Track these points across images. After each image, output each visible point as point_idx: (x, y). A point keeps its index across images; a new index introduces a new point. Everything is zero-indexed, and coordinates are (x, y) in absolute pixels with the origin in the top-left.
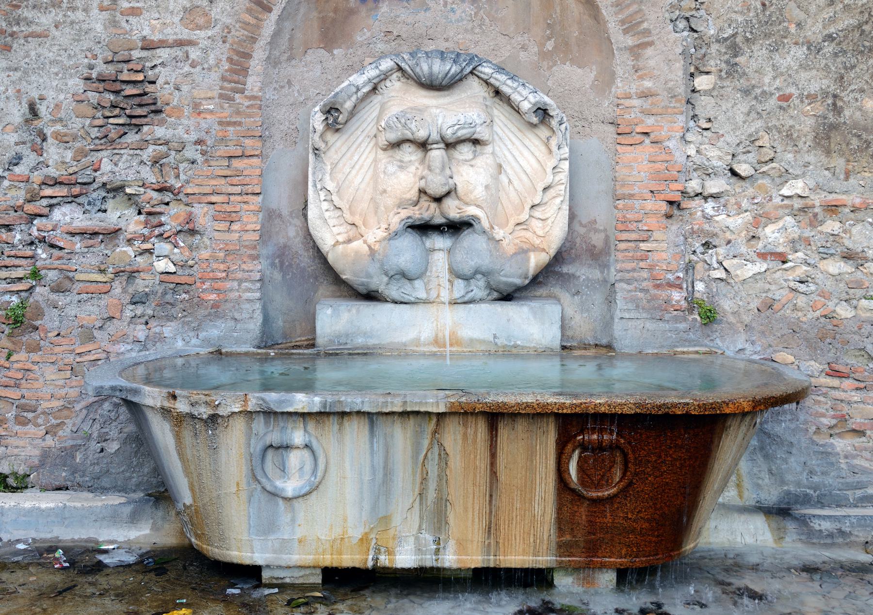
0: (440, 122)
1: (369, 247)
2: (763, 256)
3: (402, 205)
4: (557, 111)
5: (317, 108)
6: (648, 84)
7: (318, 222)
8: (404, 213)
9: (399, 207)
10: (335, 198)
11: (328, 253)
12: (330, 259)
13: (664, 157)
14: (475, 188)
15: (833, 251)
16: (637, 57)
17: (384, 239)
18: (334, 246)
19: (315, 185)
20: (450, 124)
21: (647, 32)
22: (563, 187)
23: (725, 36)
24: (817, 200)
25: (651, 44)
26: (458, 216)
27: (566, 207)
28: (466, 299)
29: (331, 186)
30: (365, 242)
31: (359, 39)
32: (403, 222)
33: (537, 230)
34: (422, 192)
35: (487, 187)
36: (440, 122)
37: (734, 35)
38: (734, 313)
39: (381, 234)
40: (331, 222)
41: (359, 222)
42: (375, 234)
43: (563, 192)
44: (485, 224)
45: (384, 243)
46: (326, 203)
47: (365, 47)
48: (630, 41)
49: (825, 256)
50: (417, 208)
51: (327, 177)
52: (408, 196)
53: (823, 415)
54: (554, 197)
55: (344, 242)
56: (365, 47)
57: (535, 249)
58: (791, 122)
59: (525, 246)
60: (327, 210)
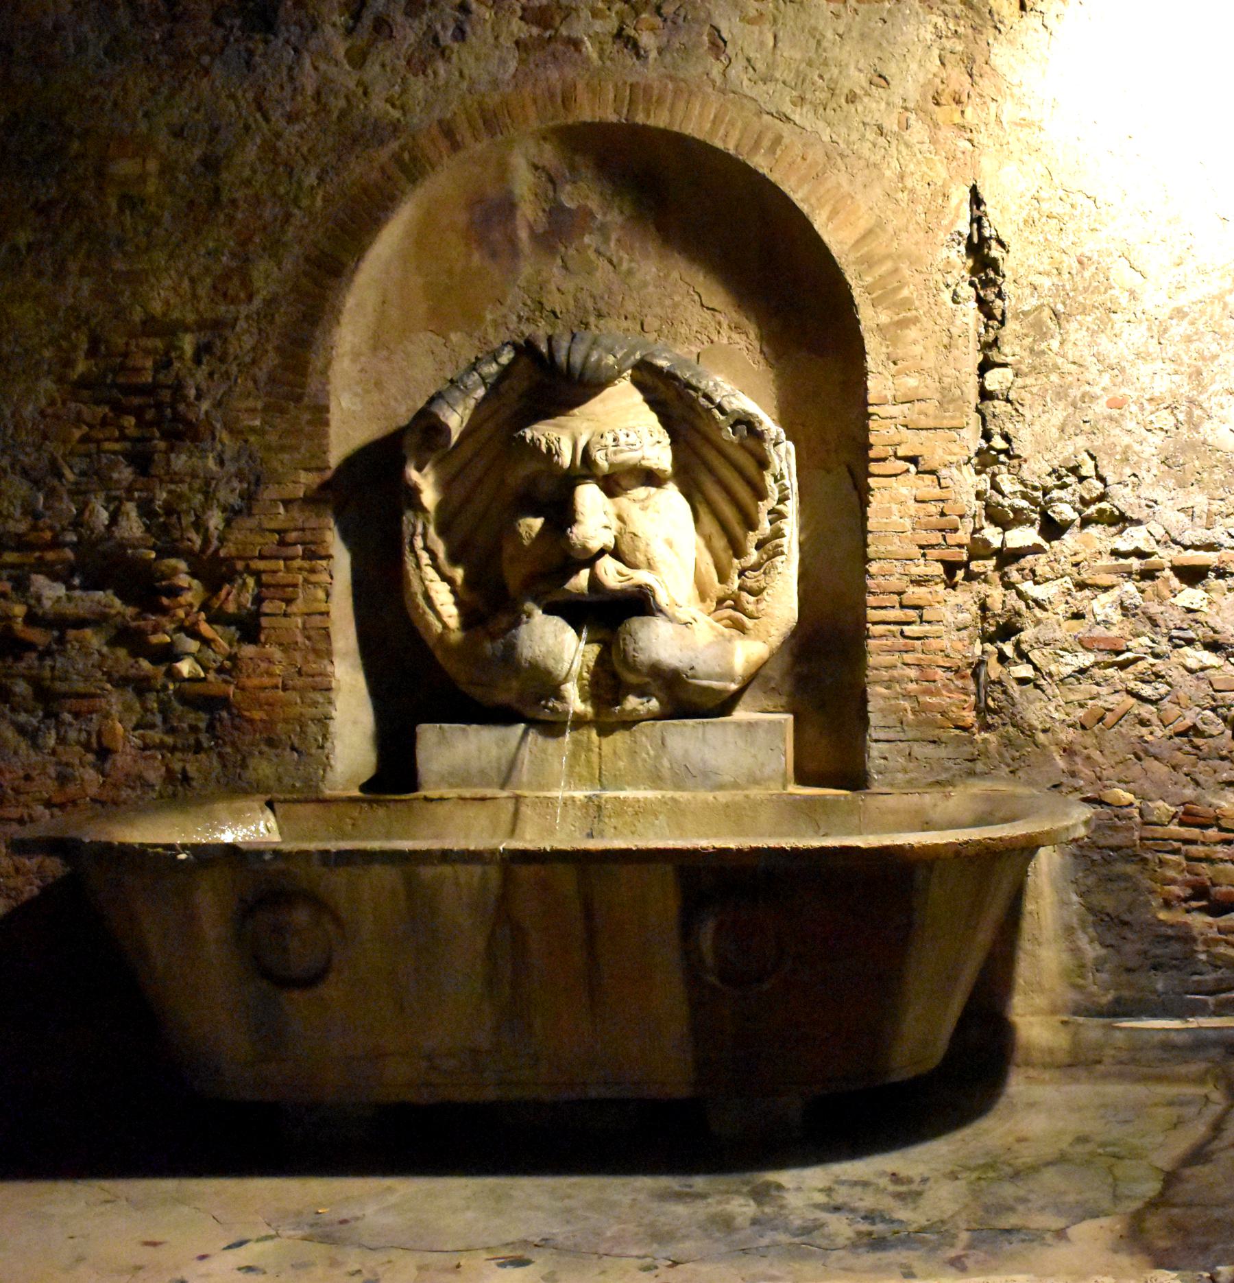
2: (1086, 645)
6: (912, 382)
13: (937, 492)
15: (1191, 634)
16: (895, 342)
21: (906, 304)
23: (1026, 308)
24: (1167, 556)
25: (916, 320)
37: (1039, 308)
38: (1045, 731)
48: (884, 318)
49: (1178, 643)
53: (1173, 882)
58: (1126, 440)
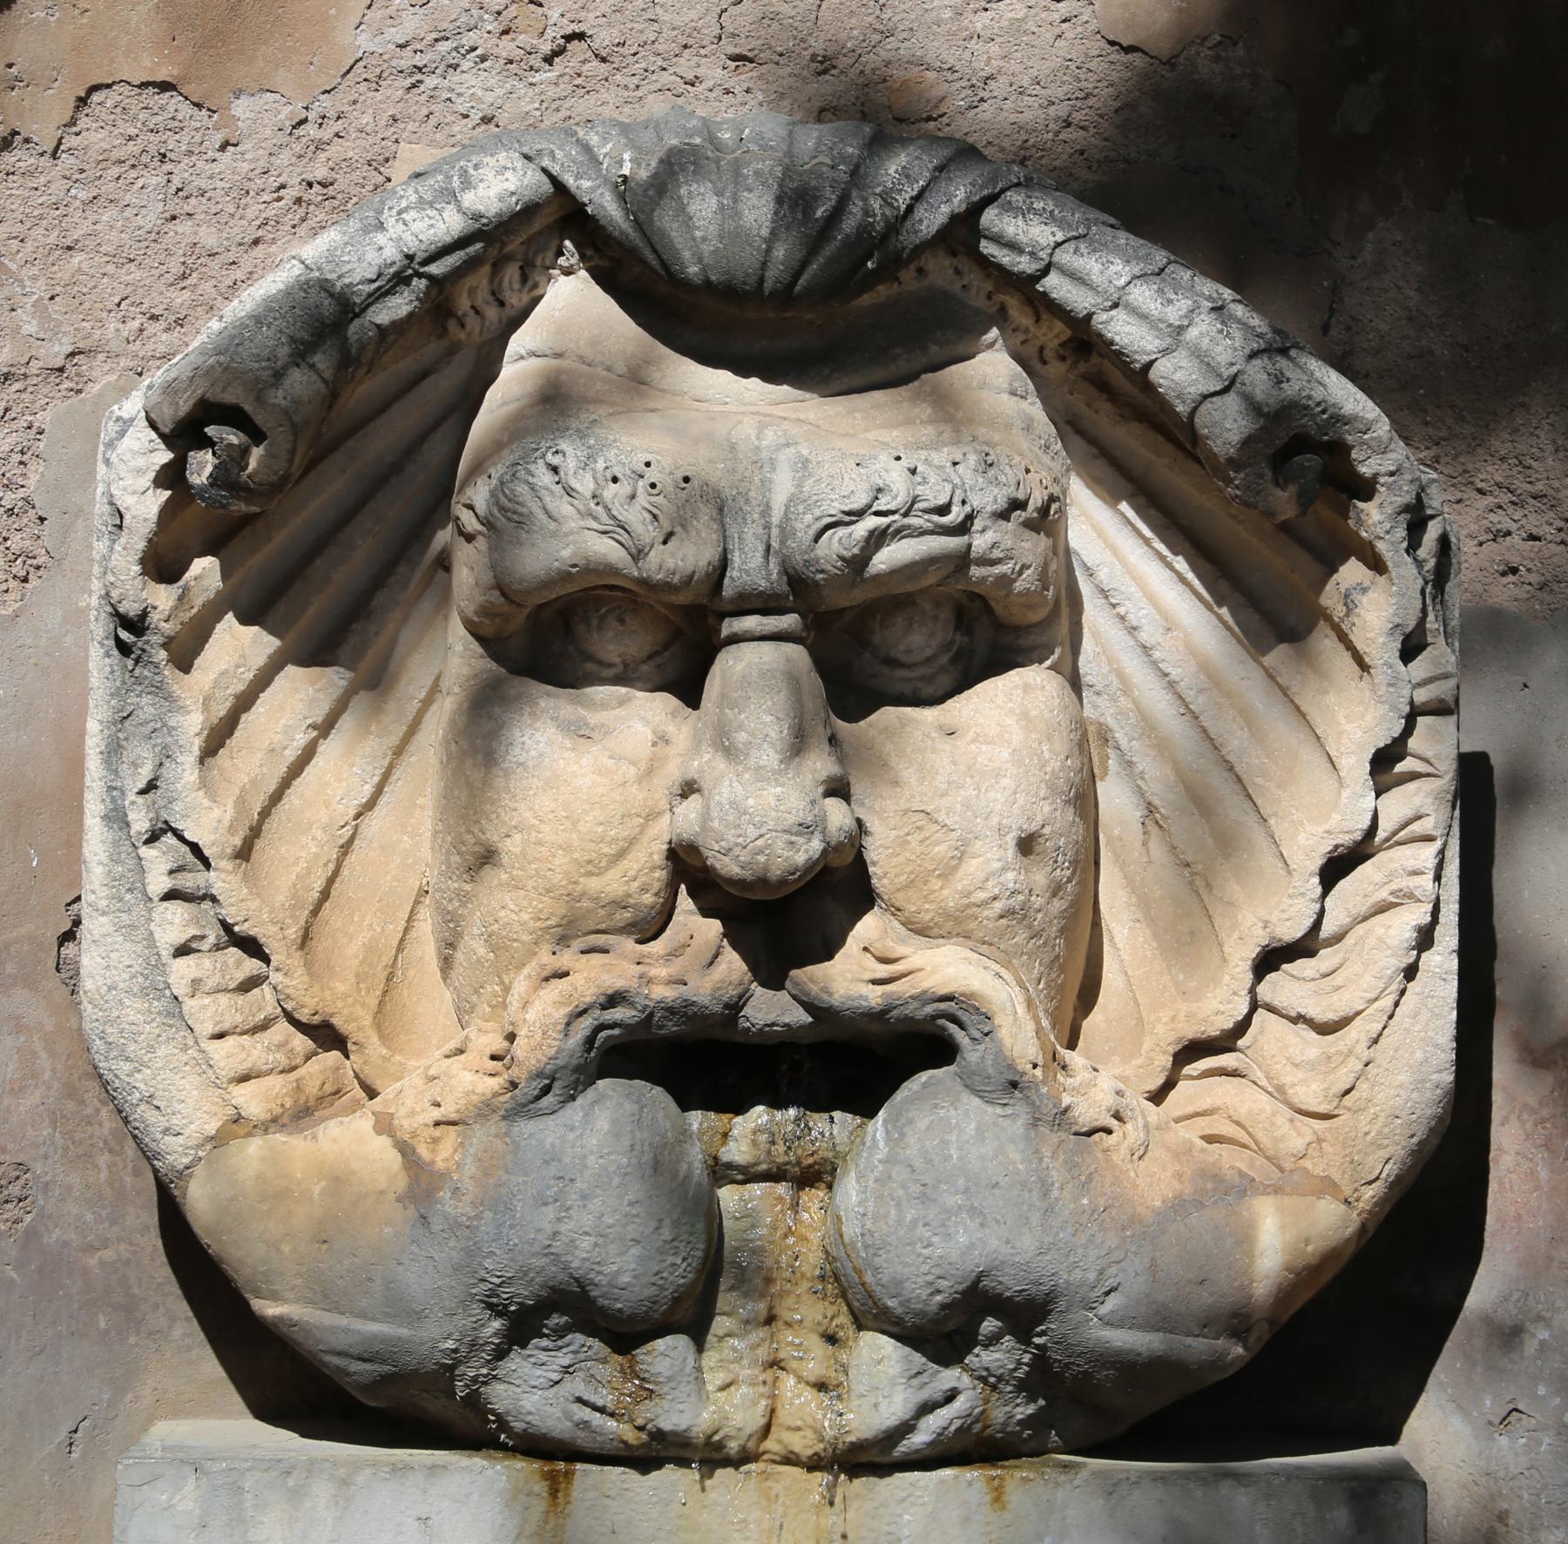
0: (779, 501)
1: (405, 1149)
3: (574, 929)
4: (1400, 452)
5: (133, 406)
7: (134, 1011)
8: (593, 976)
9: (563, 940)
10: (222, 880)
11: (184, 1174)
12: (199, 1200)
14: (962, 854)
17: (485, 1109)
18: (218, 1140)
19: (117, 818)
20: (835, 507)
22: (1426, 855)
26: (874, 997)
27: (1443, 960)
28: (920, 1438)
29: (208, 823)
30: (384, 1125)
31: (365, 41)
32: (585, 1025)
33: (1289, 1077)
34: (687, 867)
35: (1026, 845)
36: (779, 501)
39: (471, 1081)
40: (206, 1012)
41: (353, 1019)
42: (439, 1069)
43: (1427, 881)
44: (1018, 1029)
45: (483, 1135)
46: (177, 910)
47: (395, 88)
50: (656, 947)
51: (185, 771)
52: (612, 884)
54: (1383, 908)
55: (273, 1123)
56: (395, 88)
57: (1286, 1179)
59: (1229, 1160)
60: (183, 951)
